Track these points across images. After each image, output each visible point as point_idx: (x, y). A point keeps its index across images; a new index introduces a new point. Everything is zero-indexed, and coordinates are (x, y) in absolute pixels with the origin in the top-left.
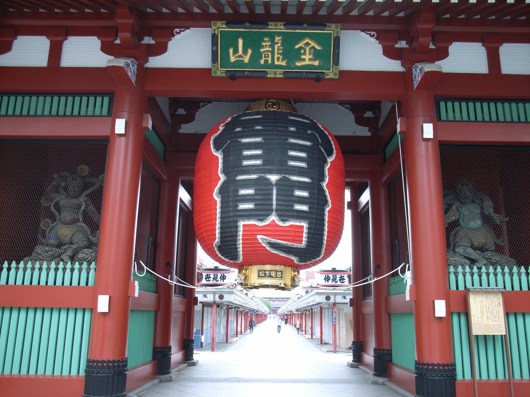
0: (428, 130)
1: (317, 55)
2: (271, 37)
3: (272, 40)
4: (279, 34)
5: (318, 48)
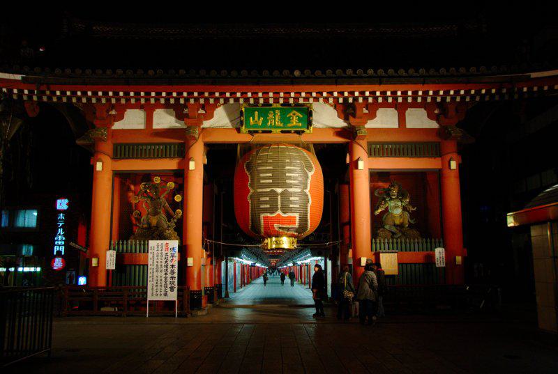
0: (361, 165)
1: (300, 120)
2: (274, 110)
3: (274, 113)
4: (278, 109)
5: (301, 116)
